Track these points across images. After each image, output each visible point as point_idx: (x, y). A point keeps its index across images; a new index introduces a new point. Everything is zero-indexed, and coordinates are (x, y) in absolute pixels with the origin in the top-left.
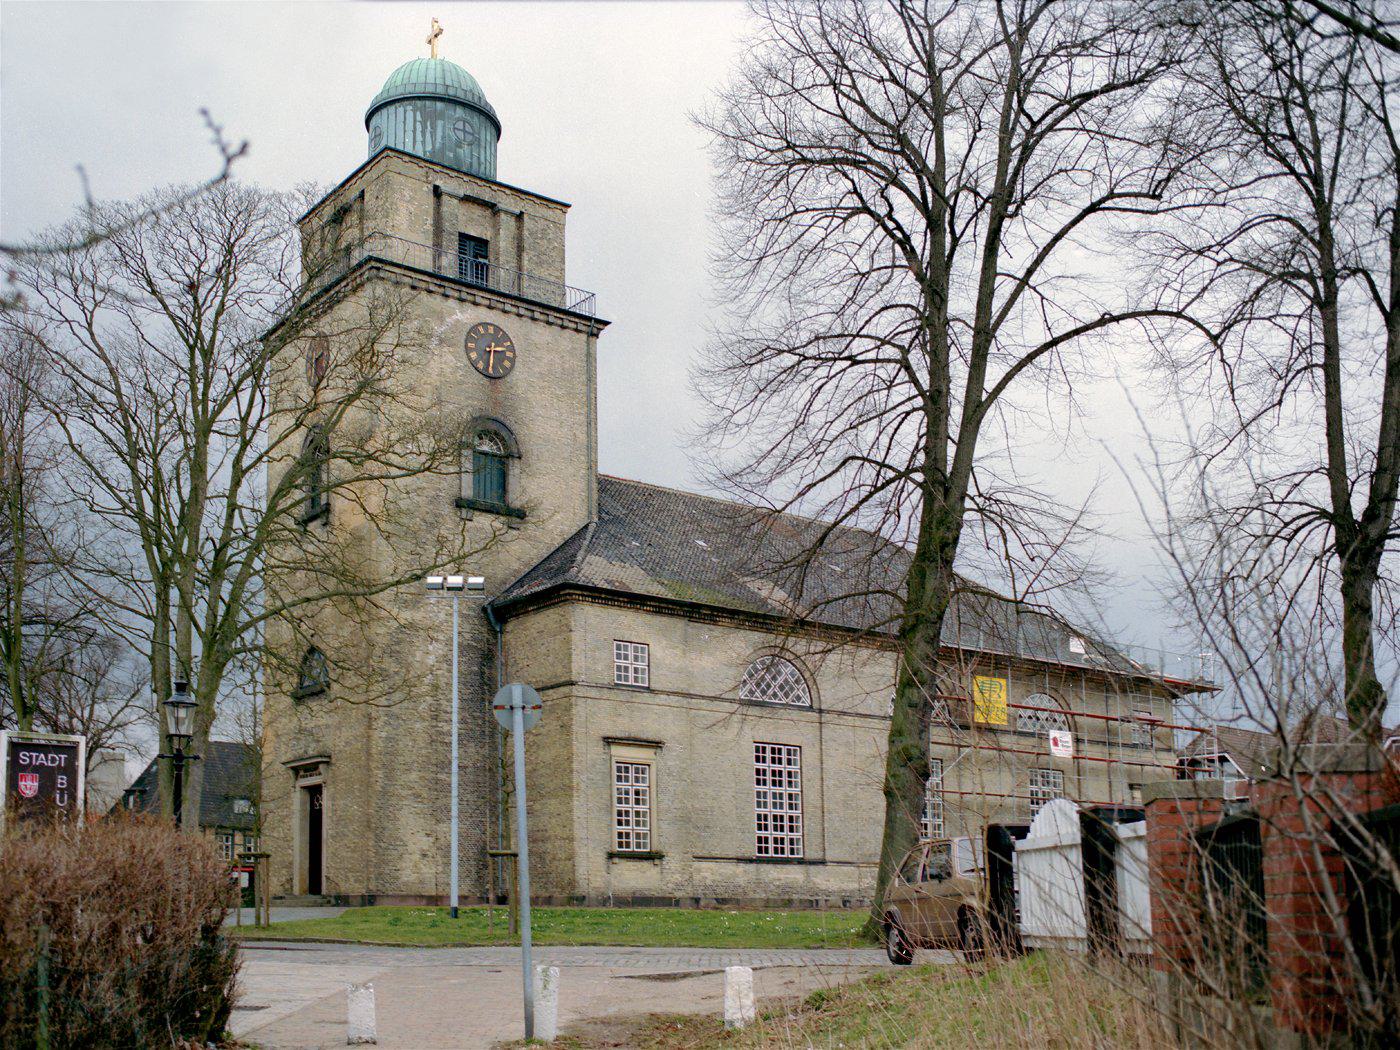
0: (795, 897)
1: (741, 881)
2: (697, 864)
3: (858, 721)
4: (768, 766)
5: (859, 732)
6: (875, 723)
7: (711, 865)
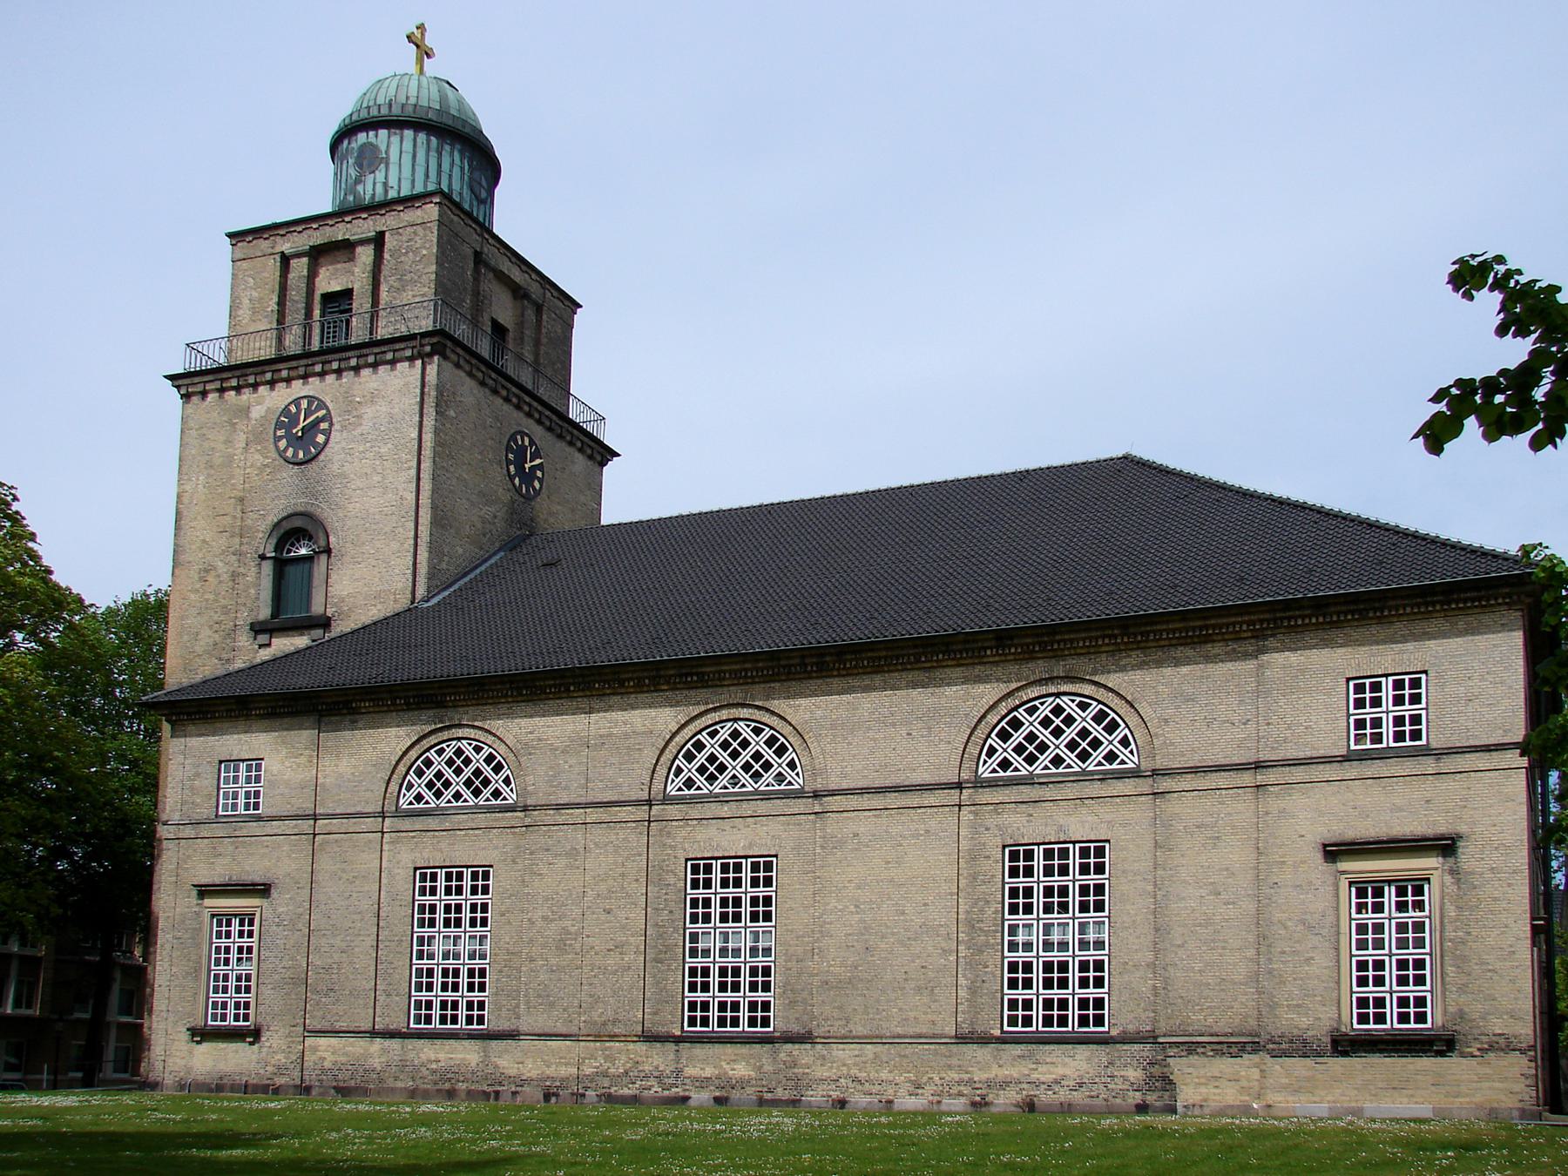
0: (462, 1086)
1: (377, 1063)
2: (309, 1041)
3: (593, 815)
4: (441, 899)
5: (598, 834)
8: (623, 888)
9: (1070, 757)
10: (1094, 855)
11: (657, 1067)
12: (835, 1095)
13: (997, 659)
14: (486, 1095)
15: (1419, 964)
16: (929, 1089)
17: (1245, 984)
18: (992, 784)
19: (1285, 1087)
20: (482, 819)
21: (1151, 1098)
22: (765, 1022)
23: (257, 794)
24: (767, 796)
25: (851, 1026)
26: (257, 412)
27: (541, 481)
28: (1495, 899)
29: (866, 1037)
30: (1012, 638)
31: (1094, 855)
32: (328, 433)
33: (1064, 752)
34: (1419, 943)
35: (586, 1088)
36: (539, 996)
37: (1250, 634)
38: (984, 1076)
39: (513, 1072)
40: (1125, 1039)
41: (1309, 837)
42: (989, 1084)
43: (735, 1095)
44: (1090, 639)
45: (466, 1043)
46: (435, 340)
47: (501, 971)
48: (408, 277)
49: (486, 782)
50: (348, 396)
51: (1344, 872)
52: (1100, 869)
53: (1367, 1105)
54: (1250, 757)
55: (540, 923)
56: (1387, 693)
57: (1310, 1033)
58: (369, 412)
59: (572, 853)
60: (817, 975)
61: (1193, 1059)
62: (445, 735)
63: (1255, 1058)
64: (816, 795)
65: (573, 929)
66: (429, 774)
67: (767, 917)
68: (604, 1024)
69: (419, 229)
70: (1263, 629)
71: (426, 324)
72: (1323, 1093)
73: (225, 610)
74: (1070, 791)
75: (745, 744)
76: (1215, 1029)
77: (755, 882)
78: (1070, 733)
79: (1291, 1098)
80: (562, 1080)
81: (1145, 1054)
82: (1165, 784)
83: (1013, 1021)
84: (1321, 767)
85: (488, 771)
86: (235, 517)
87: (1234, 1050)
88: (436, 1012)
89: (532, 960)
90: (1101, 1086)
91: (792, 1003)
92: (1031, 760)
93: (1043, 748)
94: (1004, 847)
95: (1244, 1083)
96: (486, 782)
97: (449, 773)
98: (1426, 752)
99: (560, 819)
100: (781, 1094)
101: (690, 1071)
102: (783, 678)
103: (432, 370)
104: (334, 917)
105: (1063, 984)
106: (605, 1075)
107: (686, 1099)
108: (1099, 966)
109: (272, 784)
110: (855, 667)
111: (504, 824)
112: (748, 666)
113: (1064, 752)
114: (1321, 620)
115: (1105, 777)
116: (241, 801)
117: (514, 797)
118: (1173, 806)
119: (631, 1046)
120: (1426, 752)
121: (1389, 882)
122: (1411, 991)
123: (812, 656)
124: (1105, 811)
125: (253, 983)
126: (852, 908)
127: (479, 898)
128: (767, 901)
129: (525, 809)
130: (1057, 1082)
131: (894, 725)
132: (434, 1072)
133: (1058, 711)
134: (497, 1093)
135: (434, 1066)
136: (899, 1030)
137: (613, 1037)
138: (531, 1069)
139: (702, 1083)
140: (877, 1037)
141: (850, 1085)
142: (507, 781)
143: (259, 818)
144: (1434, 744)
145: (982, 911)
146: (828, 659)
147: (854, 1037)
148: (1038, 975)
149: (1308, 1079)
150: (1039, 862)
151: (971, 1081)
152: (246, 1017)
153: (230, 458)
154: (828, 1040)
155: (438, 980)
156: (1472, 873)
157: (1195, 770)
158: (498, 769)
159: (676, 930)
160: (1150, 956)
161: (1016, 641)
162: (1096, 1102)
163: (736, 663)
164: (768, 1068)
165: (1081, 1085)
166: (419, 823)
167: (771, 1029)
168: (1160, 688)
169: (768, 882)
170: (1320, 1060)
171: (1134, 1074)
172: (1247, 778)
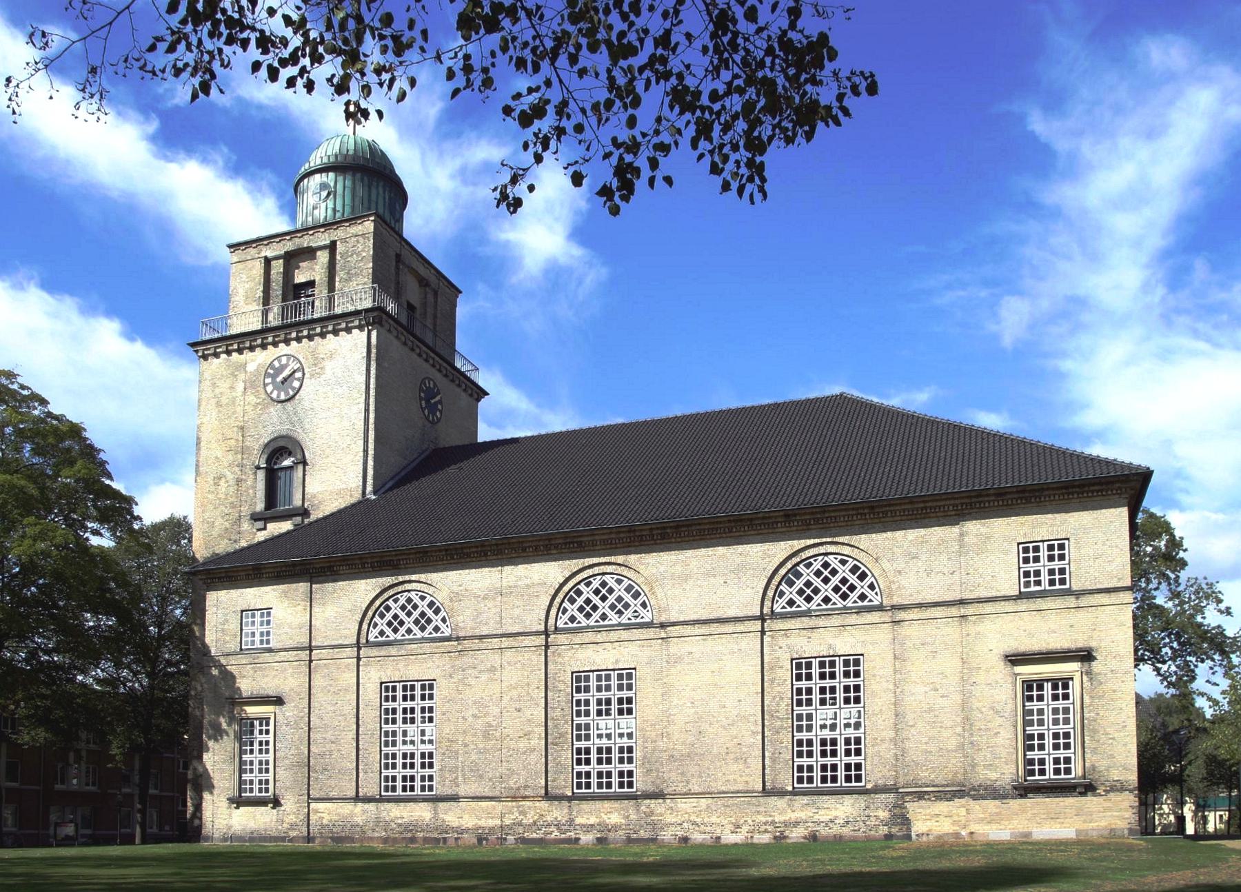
1: (359, 820)
3: (506, 642)
5: (509, 654)
6: (527, 641)
7: (329, 805)
8: (528, 694)
9: (835, 598)
10: (854, 665)
11: (556, 818)
12: (680, 834)
13: (784, 529)
14: (437, 840)
15: (1067, 735)
16: (745, 829)
17: (956, 751)
18: (783, 616)
19: (982, 820)
20: (427, 647)
21: (894, 830)
22: (630, 785)
23: (268, 633)
24: (628, 627)
25: (690, 786)
26: (251, 367)
27: (441, 412)
28: (1114, 691)
29: (701, 794)
30: (795, 515)
31: (854, 665)
32: (302, 380)
33: (831, 594)
34: (1066, 721)
35: (507, 834)
36: (472, 770)
37: (953, 513)
38: (782, 818)
39: (455, 824)
40: (877, 790)
41: (995, 651)
42: (786, 824)
43: (611, 836)
44: (848, 516)
45: (422, 804)
46: (375, 314)
47: (444, 754)
48: (353, 272)
49: (429, 621)
50: (313, 353)
51: (1019, 674)
52: (857, 674)
53: (1035, 830)
54: (957, 596)
55: (470, 719)
56: (1043, 553)
57: (998, 783)
58: (328, 365)
59: (492, 670)
60: (665, 751)
61: (922, 803)
62: (400, 588)
63: (963, 801)
64: (663, 626)
65: (494, 723)
66: (389, 616)
67: (630, 712)
68: (518, 789)
69: (360, 239)
70: (962, 509)
71: (368, 304)
72: (1007, 823)
73: (233, 505)
74: (837, 620)
75: (611, 591)
76: (937, 782)
77: (620, 688)
78: (835, 581)
79: (985, 827)
80: (490, 829)
81: (890, 800)
82: (901, 615)
83: (800, 780)
84: (1003, 603)
85: (430, 613)
86: (237, 440)
87: (948, 796)
88: (399, 784)
89: (466, 745)
90: (861, 823)
91: (649, 771)
92: (809, 599)
93: (816, 591)
94: (792, 660)
95: (955, 818)
96: (429, 621)
97: (402, 615)
98: (1069, 592)
99: (483, 646)
100: (642, 834)
101: (579, 821)
102: (637, 544)
103: (374, 334)
104: (325, 718)
105: (834, 753)
106: (520, 824)
107: (577, 840)
108: (858, 741)
109: (279, 626)
110: (688, 536)
111: (443, 650)
112: (613, 536)
113: (831, 594)
114: (1001, 503)
115: (860, 610)
116: (257, 638)
117: (449, 630)
118: (906, 630)
119: (538, 804)
120: (1069, 592)
121: (1047, 681)
122: (1062, 754)
123: (658, 528)
124: (860, 634)
125: (271, 766)
126: (689, 705)
127: (427, 703)
128: (629, 701)
129: (458, 639)
130: (832, 821)
131: (715, 576)
132: (400, 825)
133: (826, 565)
134: (445, 839)
135: (400, 821)
136: (723, 788)
137: (525, 798)
138: (469, 822)
139: (589, 828)
140: (709, 793)
141: (691, 827)
142: (444, 620)
143: (270, 650)
144: (1074, 588)
145: (778, 704)
146: (668, 531)
147: (693, 794)
148: (817, 748)
149: (997, 814)
150: (815, 671)
151: (773, 822)
152: (267, 790)
153: (234, 398)
154: (675, 795)
155: (399, 761)
156: (1099, 674)
157: (920, 606)
158: (437, 612)
159: (566, 722)
160: (892, 734)
161: (798, 518)
162: (860, 834)
163: (603, 534)
164: (633, 817)
165: (847, 822)
166: (384, 651)
167: (634, 790)
168: (895, 549)
169: (630, 687)
170: (1004, 801)
171: (883, 814)
172: (954, 611)
